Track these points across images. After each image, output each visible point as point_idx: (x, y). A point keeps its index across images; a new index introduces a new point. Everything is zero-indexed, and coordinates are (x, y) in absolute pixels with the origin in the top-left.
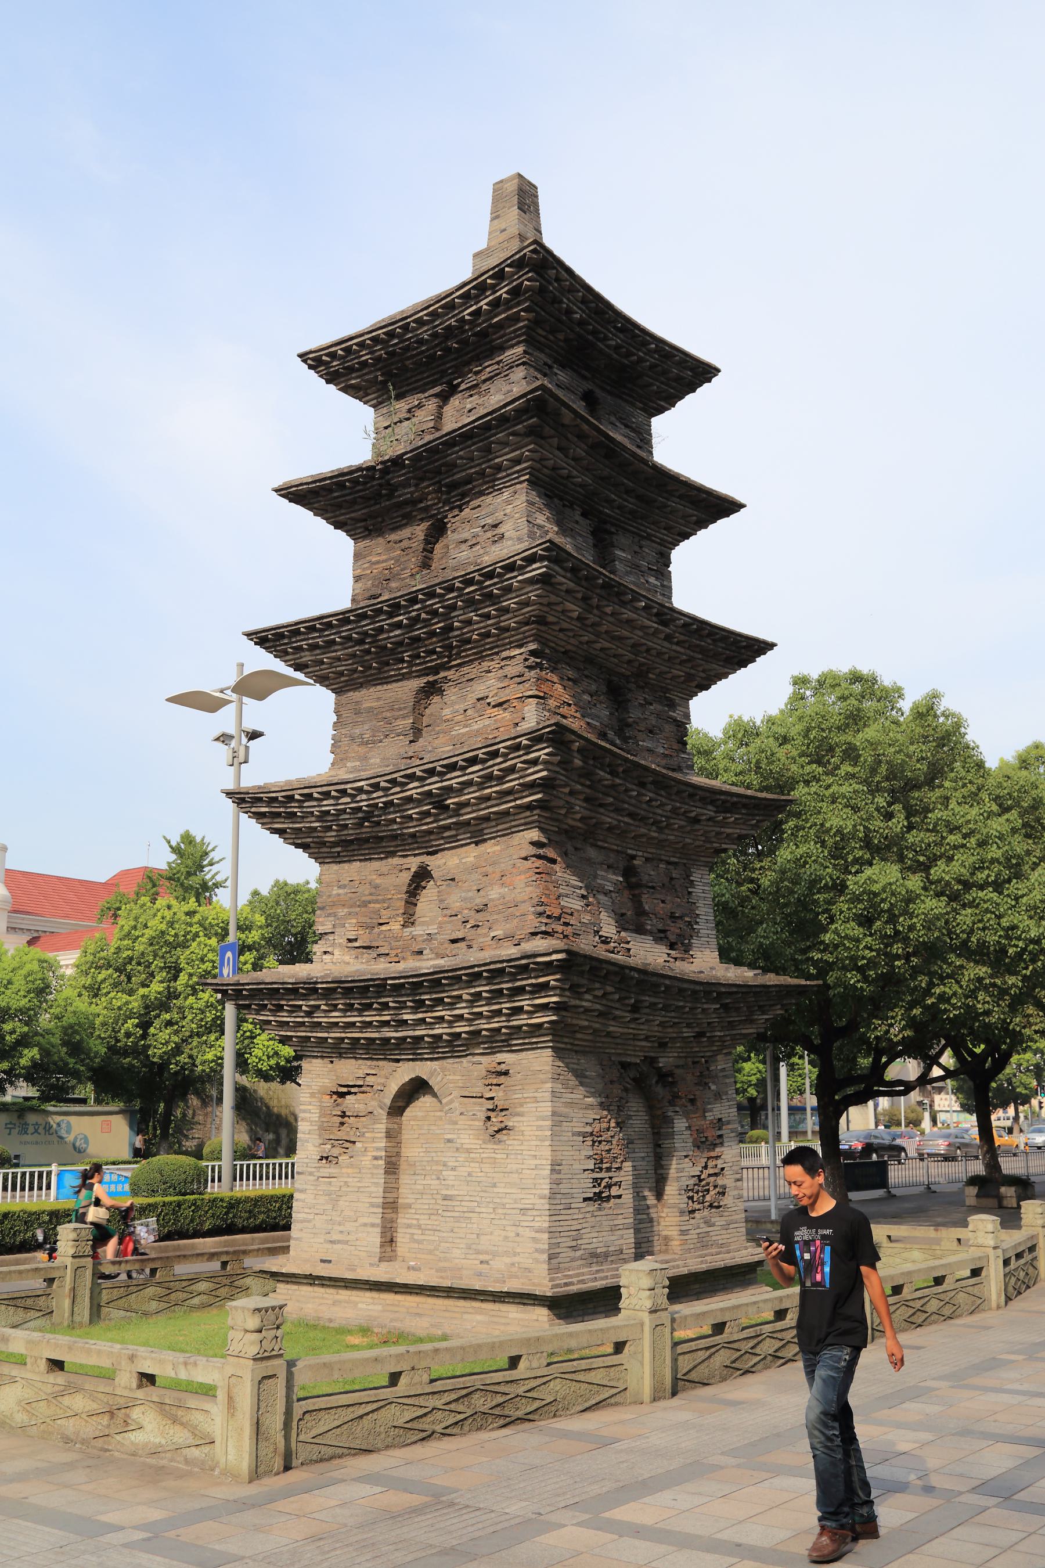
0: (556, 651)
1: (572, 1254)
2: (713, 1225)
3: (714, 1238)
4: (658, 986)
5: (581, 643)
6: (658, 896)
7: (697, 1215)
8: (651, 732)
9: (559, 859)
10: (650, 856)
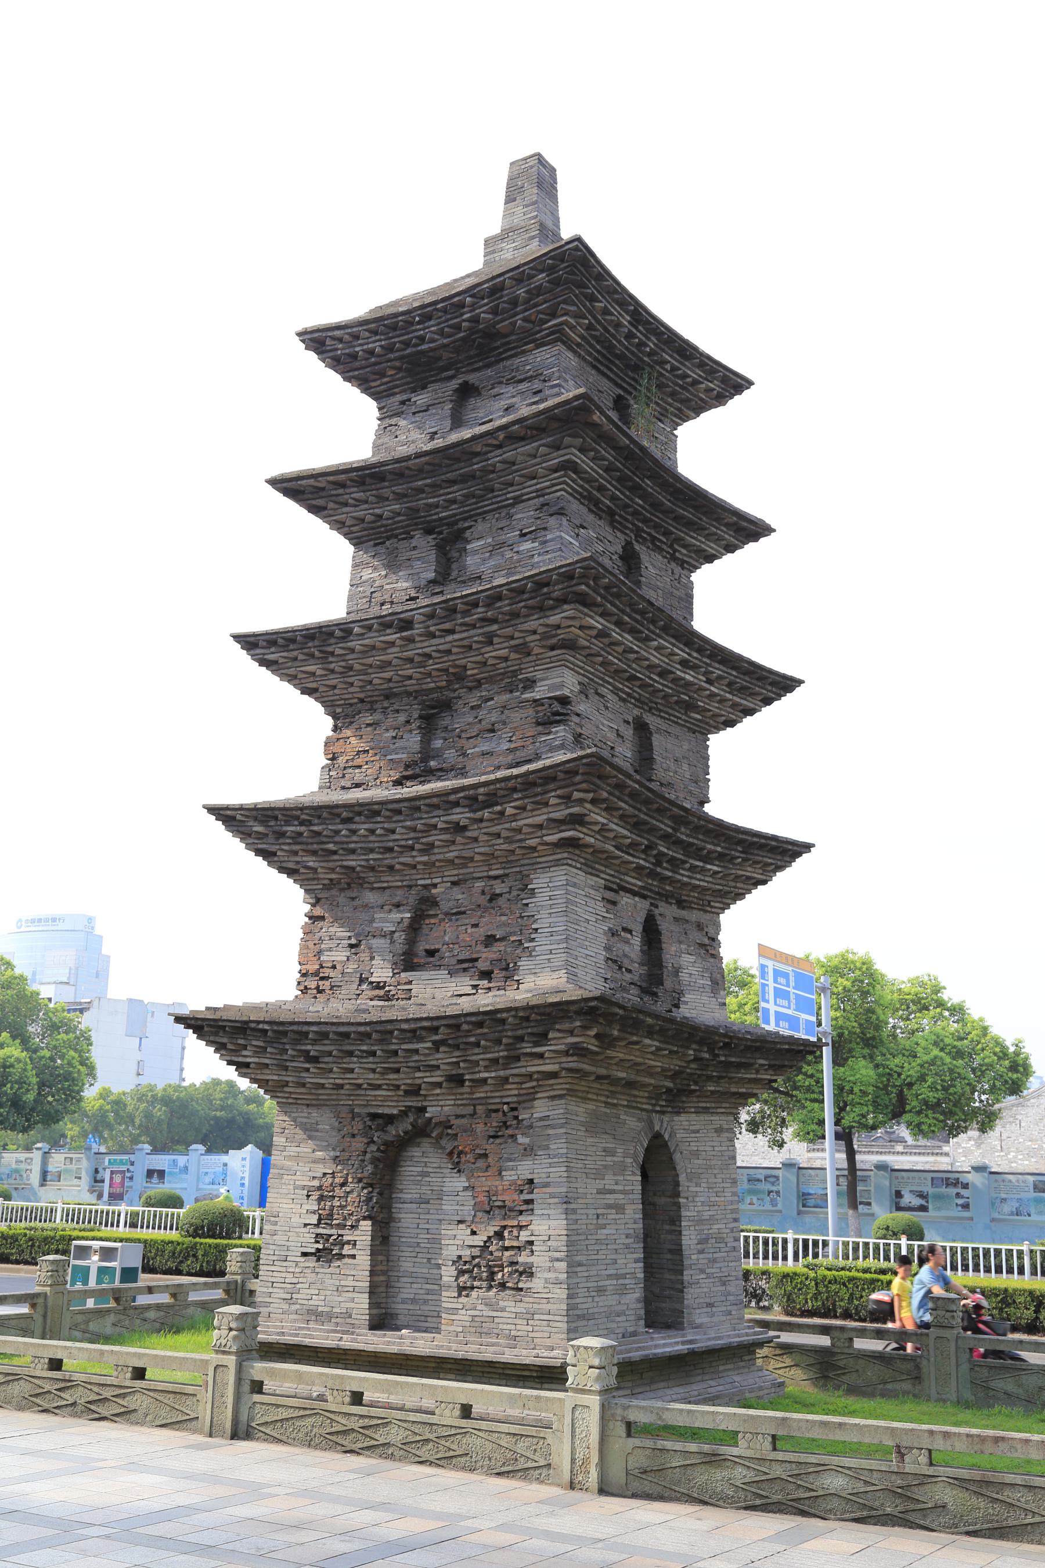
0: (351, 705)
1: (286, 1306)
2: (503, 1310)
3: (501, 1326)
4: (307, 1033)
5: (360, 687)
6: (467, 921)
7: (474, 1294)
8: (493, 731)
9: (326, 915)
10: (456, 878)
